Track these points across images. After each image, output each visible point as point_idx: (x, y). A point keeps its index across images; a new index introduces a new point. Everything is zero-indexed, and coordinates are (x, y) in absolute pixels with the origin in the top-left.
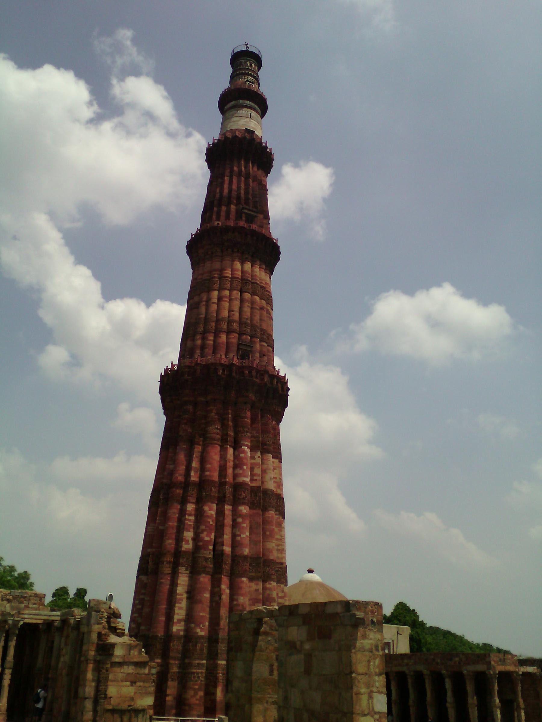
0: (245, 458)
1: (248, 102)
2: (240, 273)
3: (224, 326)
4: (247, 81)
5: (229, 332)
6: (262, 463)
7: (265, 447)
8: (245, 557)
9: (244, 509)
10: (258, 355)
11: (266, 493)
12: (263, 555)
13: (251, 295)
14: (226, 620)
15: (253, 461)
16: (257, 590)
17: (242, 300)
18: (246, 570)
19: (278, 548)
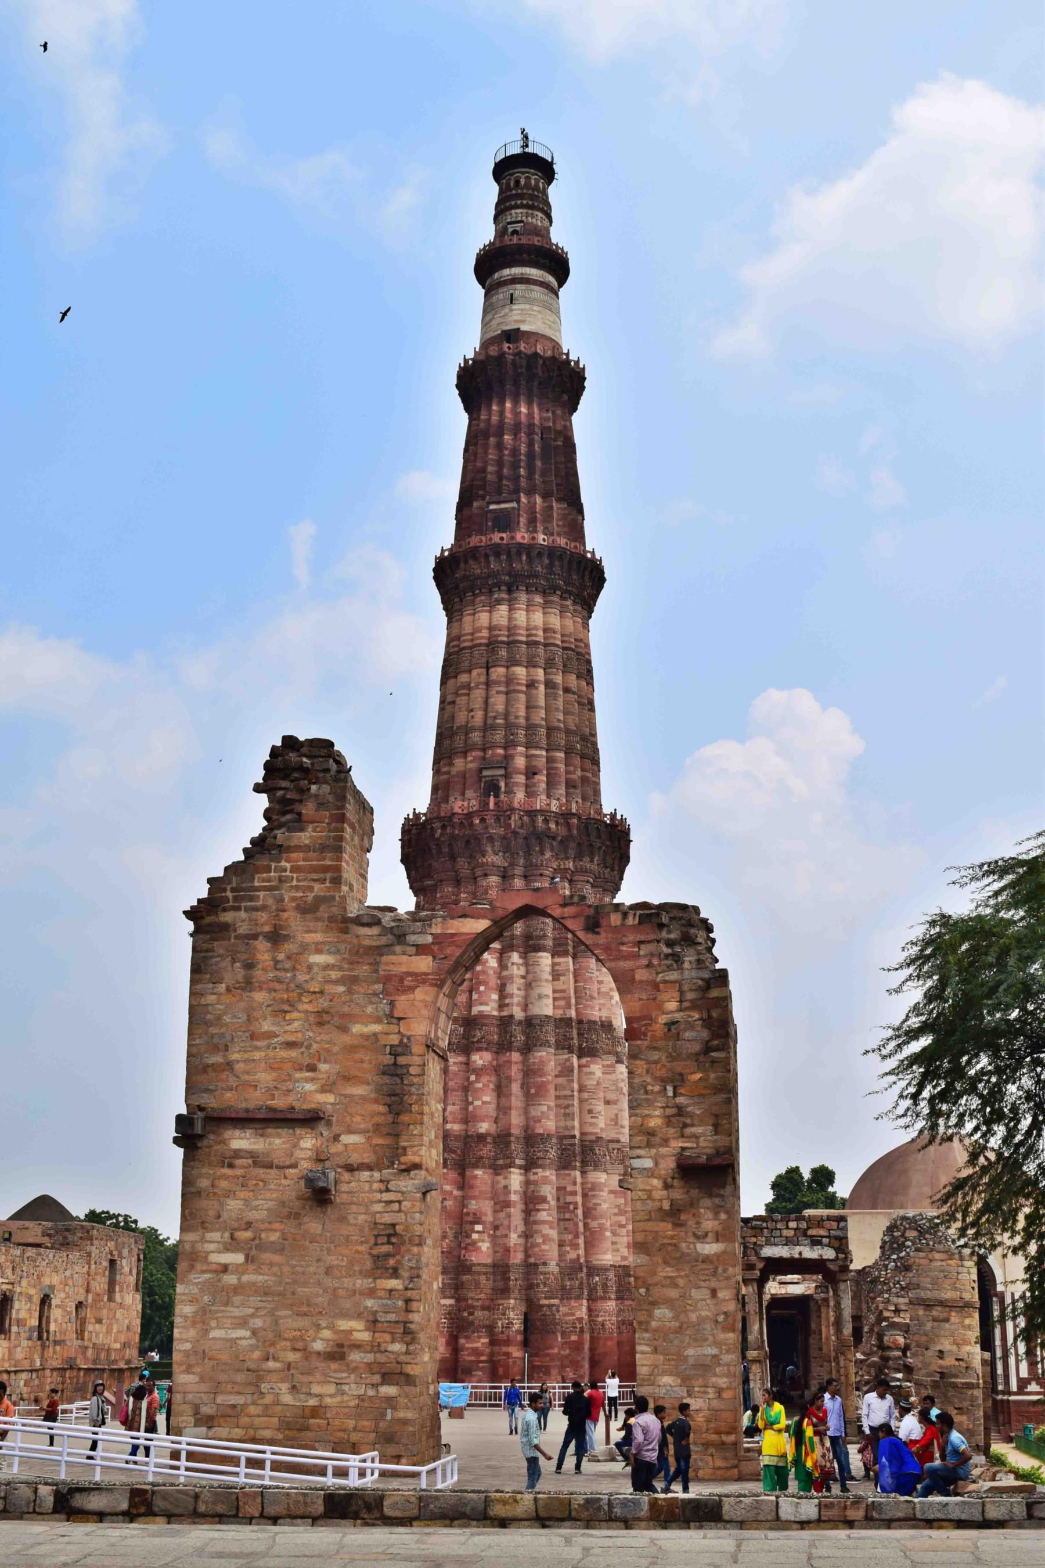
0: (484, 972)
1: (507, 272)
2: (485, 633)
3: (459, 742)
4: (509, 223)
5: (465, 754)
6: (527, 972)
7: (531, 942)
8: (481, 1138)
9: (480, 1059)
10: (521, 779)
11: (530, 1023)
12: (527, 1128)
13: (508, 667)
14: (455, 1237)
15: (505, 973)
16: (506, 1187)
17: (488, 684)
18: (482, 1158)
19: (567, 1111)
